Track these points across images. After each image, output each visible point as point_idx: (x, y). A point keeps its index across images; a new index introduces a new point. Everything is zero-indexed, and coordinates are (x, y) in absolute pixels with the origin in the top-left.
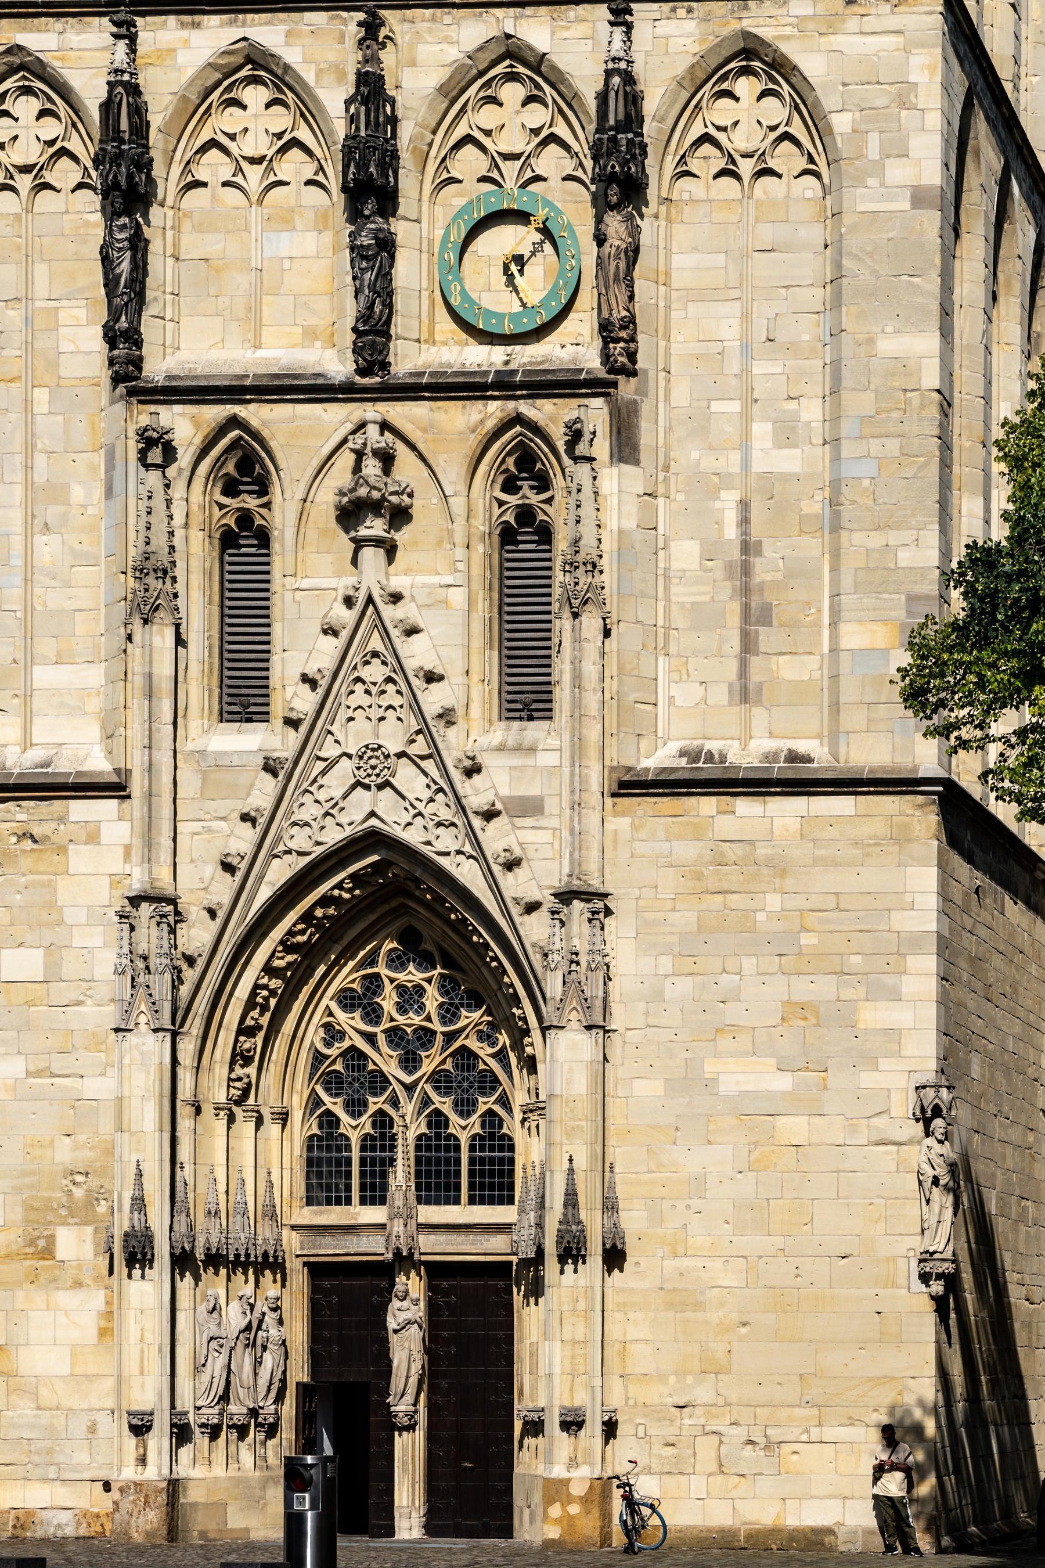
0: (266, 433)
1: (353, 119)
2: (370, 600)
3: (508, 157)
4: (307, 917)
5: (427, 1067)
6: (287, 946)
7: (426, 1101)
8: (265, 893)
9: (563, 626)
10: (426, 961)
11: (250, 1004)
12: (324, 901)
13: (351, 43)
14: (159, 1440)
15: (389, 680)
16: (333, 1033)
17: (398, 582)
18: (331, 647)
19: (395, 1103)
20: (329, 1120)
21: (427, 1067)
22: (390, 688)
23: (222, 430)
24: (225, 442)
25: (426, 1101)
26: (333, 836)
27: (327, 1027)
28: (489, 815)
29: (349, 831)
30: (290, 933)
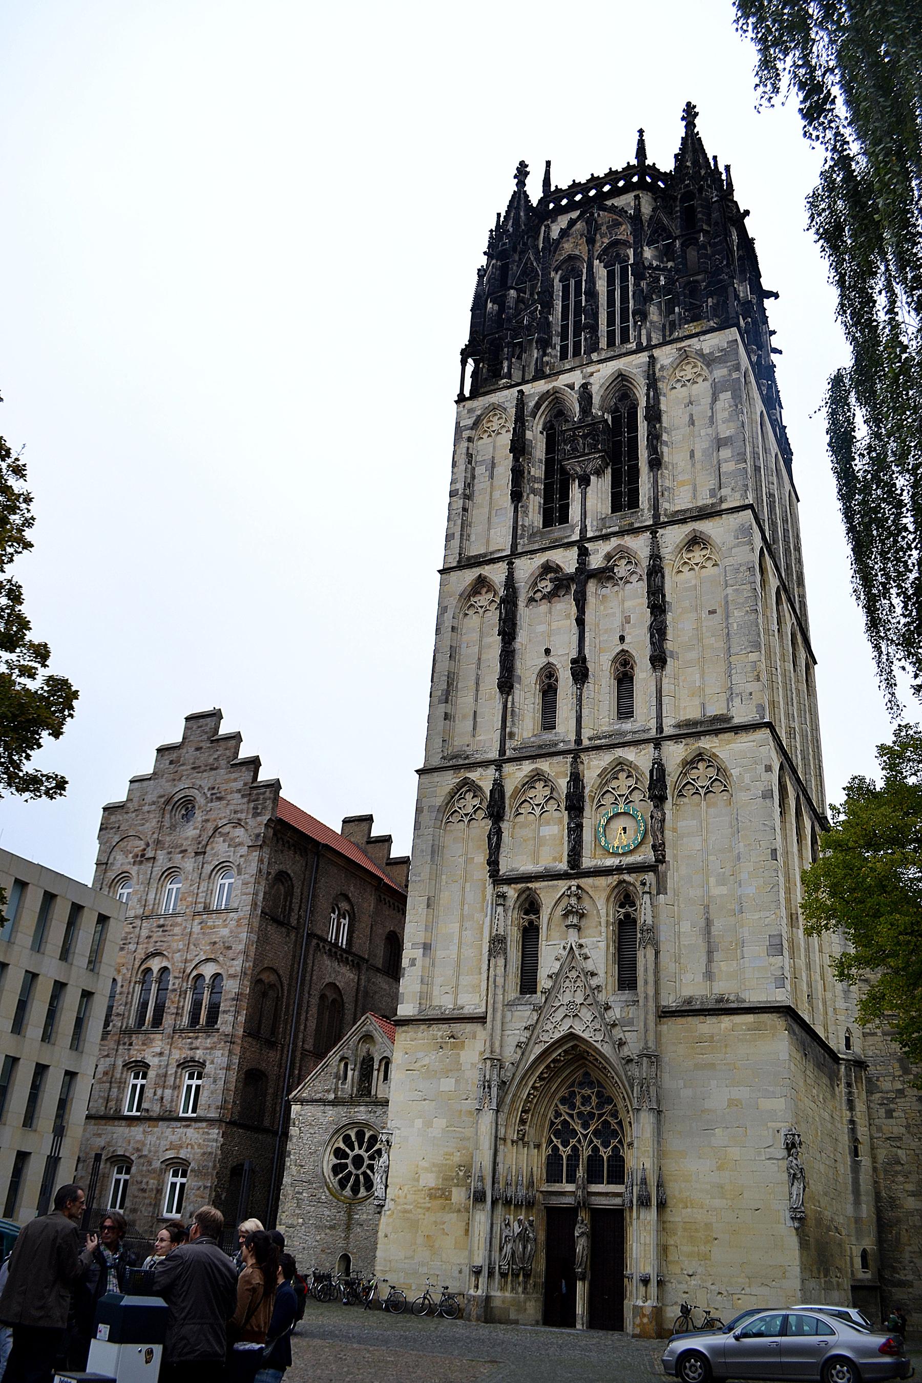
0: (538, 892)
1: (569, 788)
2: (571, 948)
3: (619, 796)
4: (548, 1067)
5: (592, 1128)
6: (541, 1078)
7: (591, 1141)
8: (532, 1057)
9: (640, 954)
10: (591, 1085)
11: (527, 1101)
12: (554, 1061)
13: (569, 765)
14: (483, 1280)
15: (578, 976)
16: (558, 1114)
17: (582, 941)
18: (557, 965)
19: (579, 1141)
20: (555, 1148)
21: (592, 1128)
22: (579, 980)
23: (524, 891)
24: (524, 896)
25: (591, 1141)
26: (557, 1036)
27: (556, 1112)
28: (614, 1025)
29: (562, 1033)
30: (542, 1073)
